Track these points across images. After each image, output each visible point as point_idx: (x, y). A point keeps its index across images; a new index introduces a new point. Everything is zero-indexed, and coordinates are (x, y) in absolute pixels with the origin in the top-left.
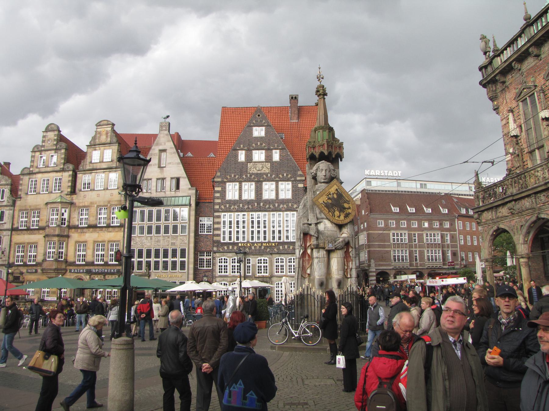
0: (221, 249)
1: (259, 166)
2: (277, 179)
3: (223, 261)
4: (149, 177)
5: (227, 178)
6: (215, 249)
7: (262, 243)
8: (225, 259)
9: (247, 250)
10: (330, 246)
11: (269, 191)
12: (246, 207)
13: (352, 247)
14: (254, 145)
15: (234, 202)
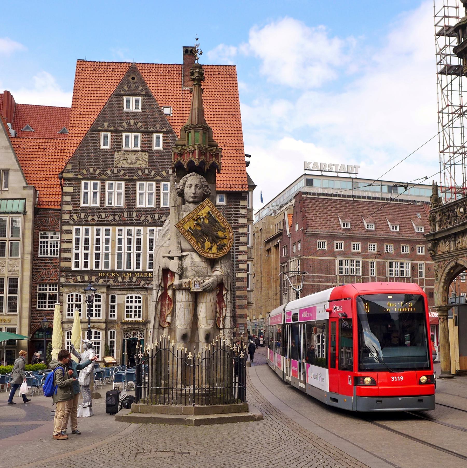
0: (71, 281)
1: (132, 157)
2: (158, 178)
3: (74, 298)
5: (82, 174)
6: (62, 280)
7: (133, 272)
8: (77, 296)
9: (111, 282)
11: (145, 194)
12: (111, 218)
13: (226, 290)
14: (124, 124)
15: (93, 211)
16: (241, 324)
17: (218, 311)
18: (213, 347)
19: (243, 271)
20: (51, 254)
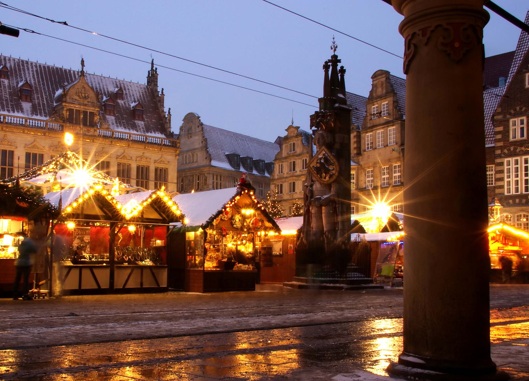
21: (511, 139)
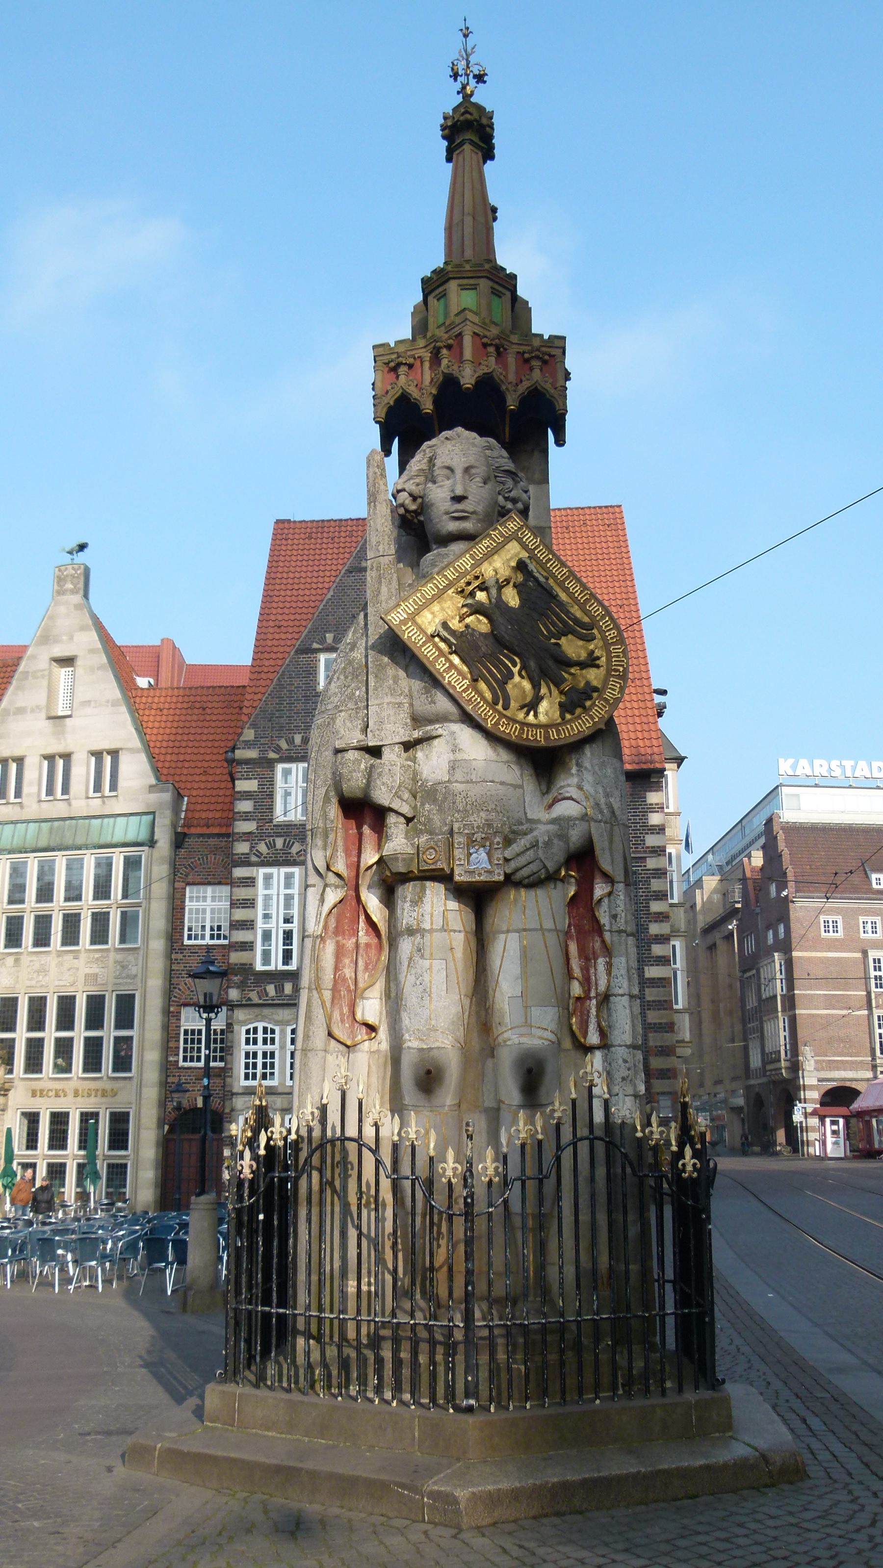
3: (260, 1036)
4: (17, 753)
5: (278, 749)
8: (265, 1030)
10: (477, 865)
13: (608, 879)
16: (663, 1093)
17: (577, 972)
18: (558, 1126)
19: (664, 961)
20: (212, 937)
21: (279, 815)
